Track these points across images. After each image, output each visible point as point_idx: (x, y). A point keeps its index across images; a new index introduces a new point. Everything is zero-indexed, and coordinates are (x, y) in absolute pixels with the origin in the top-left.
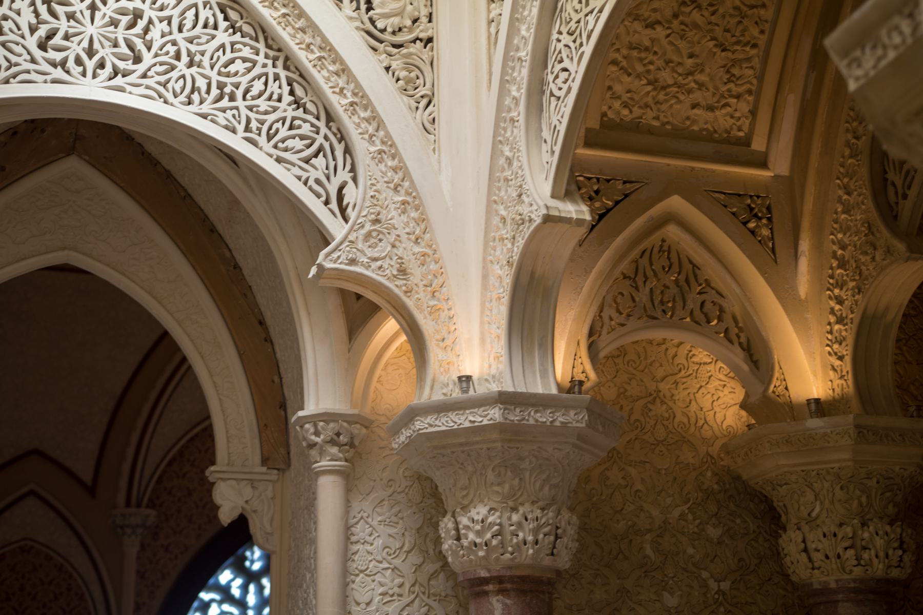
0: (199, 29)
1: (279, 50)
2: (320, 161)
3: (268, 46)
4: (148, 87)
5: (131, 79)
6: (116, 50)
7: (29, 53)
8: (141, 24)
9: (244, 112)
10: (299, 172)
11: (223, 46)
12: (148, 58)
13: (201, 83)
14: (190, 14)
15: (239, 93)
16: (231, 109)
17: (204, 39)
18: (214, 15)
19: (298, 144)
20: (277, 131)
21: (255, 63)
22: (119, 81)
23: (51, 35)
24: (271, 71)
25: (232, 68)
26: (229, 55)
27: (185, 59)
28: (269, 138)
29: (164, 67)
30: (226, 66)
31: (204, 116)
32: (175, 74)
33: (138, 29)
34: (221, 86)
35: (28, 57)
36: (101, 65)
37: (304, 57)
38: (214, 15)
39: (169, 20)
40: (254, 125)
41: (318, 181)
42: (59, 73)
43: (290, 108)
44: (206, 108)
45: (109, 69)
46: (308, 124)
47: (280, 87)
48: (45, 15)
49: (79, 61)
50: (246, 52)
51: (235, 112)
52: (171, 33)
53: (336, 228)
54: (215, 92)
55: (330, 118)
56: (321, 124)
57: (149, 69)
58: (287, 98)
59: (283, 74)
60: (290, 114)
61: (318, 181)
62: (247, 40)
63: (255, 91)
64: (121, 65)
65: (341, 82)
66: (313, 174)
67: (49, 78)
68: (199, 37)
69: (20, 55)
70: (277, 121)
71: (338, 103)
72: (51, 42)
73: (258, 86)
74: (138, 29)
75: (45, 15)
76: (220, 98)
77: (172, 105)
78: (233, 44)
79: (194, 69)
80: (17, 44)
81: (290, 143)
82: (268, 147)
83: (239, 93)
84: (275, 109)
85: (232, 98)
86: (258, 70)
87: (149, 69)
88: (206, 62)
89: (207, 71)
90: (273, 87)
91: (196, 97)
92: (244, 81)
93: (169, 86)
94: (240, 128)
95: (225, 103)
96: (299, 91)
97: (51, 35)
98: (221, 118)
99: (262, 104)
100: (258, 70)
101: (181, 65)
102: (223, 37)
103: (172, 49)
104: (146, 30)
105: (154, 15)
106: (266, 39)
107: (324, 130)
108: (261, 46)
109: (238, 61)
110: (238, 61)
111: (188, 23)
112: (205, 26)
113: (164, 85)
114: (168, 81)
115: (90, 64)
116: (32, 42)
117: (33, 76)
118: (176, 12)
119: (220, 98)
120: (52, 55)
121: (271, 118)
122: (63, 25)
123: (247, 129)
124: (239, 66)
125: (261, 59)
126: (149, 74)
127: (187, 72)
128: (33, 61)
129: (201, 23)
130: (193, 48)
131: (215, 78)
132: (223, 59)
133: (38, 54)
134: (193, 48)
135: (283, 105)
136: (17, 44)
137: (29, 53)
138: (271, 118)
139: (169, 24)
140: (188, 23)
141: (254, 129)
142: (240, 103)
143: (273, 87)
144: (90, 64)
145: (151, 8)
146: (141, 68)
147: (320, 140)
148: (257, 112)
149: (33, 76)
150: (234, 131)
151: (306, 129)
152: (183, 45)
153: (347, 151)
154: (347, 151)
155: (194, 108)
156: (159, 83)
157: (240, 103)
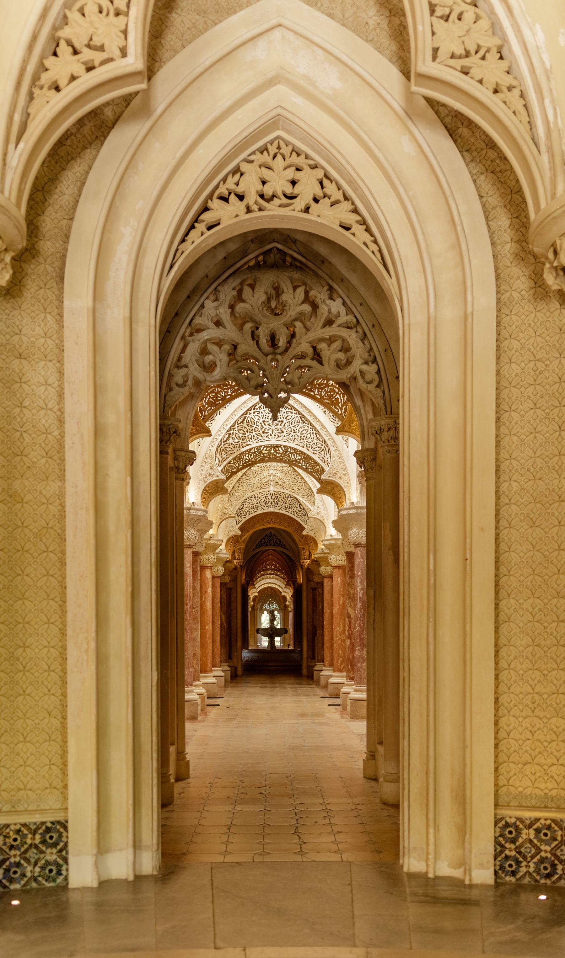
5: (282, 438)
12: (285, 432)
13: (296, 437)
15: (305, 438)
24: (312, 432)
25: (303, 432)
26: (302, 429)
27: (293, 431)
34: (301, 437)
36: (275, 436)
37: (319, 428)
42: (267, 439)
44: (298, 443)
45: (277, 436)
49: (271, 435)
50: (306, 428)
55: (325, 442)
56: (323, 443)
58: (315, 438)
59: (314, 432)
60: (316, 442)
64: (280, 435)
71: (326, 438)
73: (309, 436)
75: (263, 426)
81: (316, 449)
83: (305, 438)
85: (303, 439)
86: (309, 432)
88: (297, 431)
89: (298, 434)
90: (312, 436)
94: (305, 446)
95: (302, 441)
96: (318, 436)
98: (301, 445)
99: (310, 440)
100: (309, 432)
101: (292, 433)
103: (290, 429)
107: (324, 445)
115: (273, 435)
116: (261, 432)
117: (262, 440)
121: (311, 444)
122: (267, 427)
124: (305, 432)
125: (309, 429)
127: (294, 434)
128: (262, 436)
130: (295, 428)
131: (299, 435)
133: (263, 435)
134: (295, 428)
135: (314, 440)
138: (311, 444)
143: (312, 436)
144: (273, 435)
146: (283, 434)
147: (323, 447)
150: (303, 447)
151: (320, 445)
152: (292, 428)
155: (295, 443)
157: (305, 440)
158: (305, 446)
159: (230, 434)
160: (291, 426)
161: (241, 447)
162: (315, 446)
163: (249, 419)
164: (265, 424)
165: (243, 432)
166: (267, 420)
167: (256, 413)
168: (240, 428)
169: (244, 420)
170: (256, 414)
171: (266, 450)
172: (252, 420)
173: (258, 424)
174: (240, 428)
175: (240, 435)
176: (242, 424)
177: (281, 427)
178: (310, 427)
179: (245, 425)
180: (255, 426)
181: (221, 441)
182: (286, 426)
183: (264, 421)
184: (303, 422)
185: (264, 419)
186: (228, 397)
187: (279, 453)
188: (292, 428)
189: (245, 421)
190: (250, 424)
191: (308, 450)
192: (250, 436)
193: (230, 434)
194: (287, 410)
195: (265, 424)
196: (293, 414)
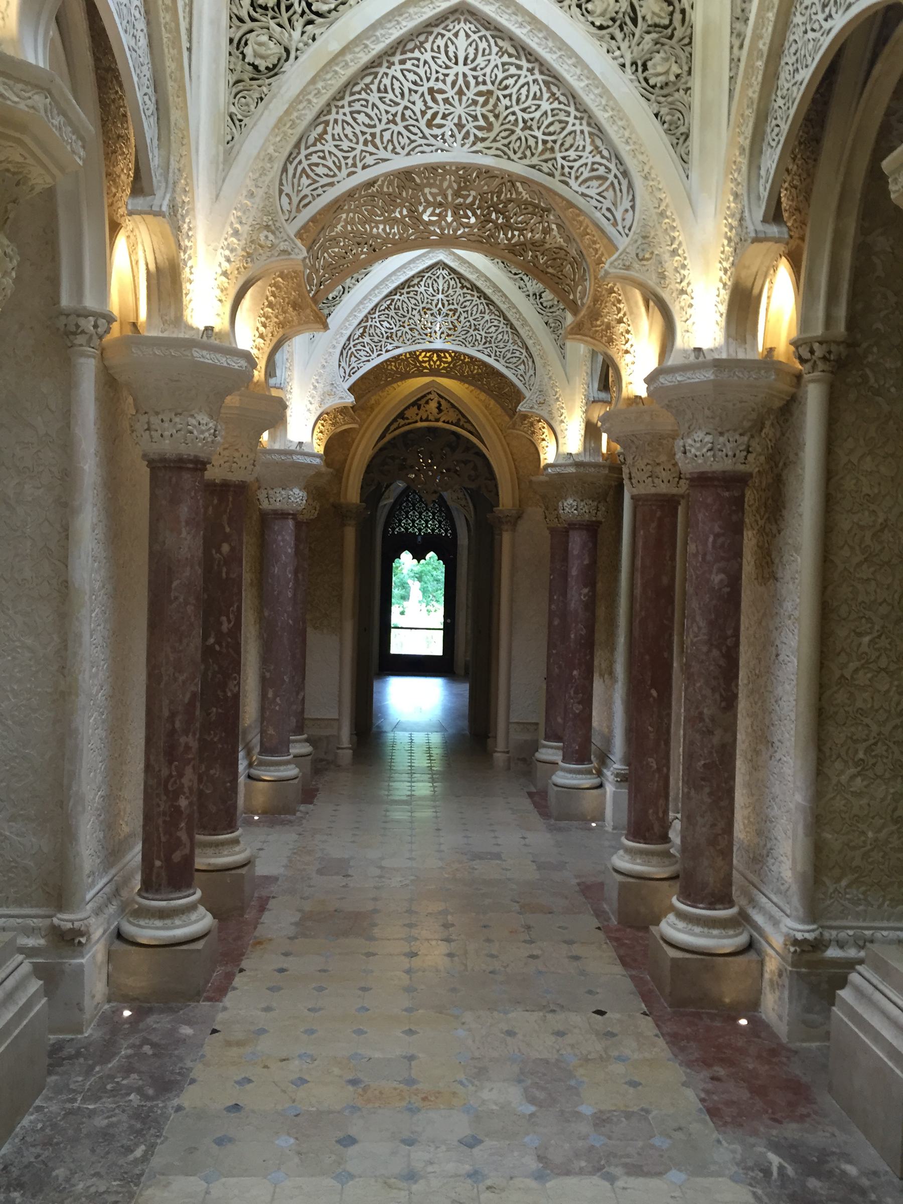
0: (478, 315)
1: (585, 111)
2: (522, 367)
3: (577, 109)
4: (497, 149)
6: (476, 123)
7: (422, 132)
8: (457, 314)
9: (495, 348)
10: (514, 371)
11: (546, 113)
13: (479, 337)
14: (475, 309)
16: (551, 159)
17: (534, 108)
18: (540, 90)
19: (514, 360)
20: (582, 173)
21: (567, 123)
22: (479, 146)
23: (435, 115)
25: (490, 330)
26: (490, 325)
27: (473, 327)
28: (504, 357)
29: (507, 133)
30: (547, 127)
31: (533, 167)
32: (469, 335)
33: (490, 107)
34: (486, 337)
35: (421, 135)
38: (540, 90)
39: (510, 95)
40: (498, 353)
41: (521, 375)
43: (590, 156)
44: (480, 348)
46: (603, 167)
47: (584, 140)
48: (430, 103)
50: (496, 323)
51: (553, 161)
52: (511, 106)
53: (527, 394)
54: (484, 340)
56: (524, 351)
57: (498, 135)
60: (512, 348)
61: (521, 375)
62: (562, 106)
63: (567, 145)
65: (530, 334)
66: (520, 372)
67: (433, 148)
68: (530, 107)
69: (416, 134)
70: (582, 166)
72: (434, 122)
73: (500, 336)
74: (456, 317)
76: (485, 343)
77: (513, 160)
78: (552, 110)
79: (476, 332)
80: (414, 126)
81: (511, 360)
82: (502, 361)
84: (581, 157)
86: (500, 330)
87: (498, 135)
89: (481, 332)
90: (506, 337)
91: (476, 343)
92: (494, 335)
93: (511, 146)
94: (493, 355)
95: (487, 345)
97: (435, 115)
98: (486, 351)
99: (501, 345)
100: (500, 330)
102: (487, 317)
103: (468, 324)
104: (459, 317)
105: (461, 310)
106: (575, 104)
108: (501, 319)
109: (556, 124)
110: (556, 124)
111: (474, 313)
112: (481, 313)
113: (507, 146)
114: (510, 143)
118: (469, 309)
119: (485, 343)
120: (436, 131)
123: (496, 356)
124: (493, 329)
126: (498, 138)
129: (531, 95)
130: (476, 323)
132: (487, 326)
134: (476, 323)
135: (509, 344)
136: (414, 126)
137: (422, 132)
138: (504, 350)
139: (510, 100)
140: (474, 313)
141: (567, 174)
142: (493, 345)
145: (498, 89)
148: (569, 161)
149: (425, 148)
150: (490, 356)
152: (473, 322)
153: (533, 362)
154: (533, 362)
155: (475, 348)
156: (504, 145)
157: (493, 345)
158: (493, 355)
159: (366, 327)
160: (470, 319)
161: (384, 350)
162: (509, 355)
163: (399, 304)
164: (434, 100)
165: (388, 326)
166: (440, 85)
167: (408, 65)
168: (383, 318)
169: (391, 304)
170: (412, 294)
171: (425, 356)
172: (405, 305)
173: (415, 312)
174: (383, 318)
175: (383, 330)
176: (387, 312)
177: (484, 110)
178: (502, 321)
179: (392, 313)
180: (409, 315)
181: (349, 339)
182: (462, 318)
183: (431, 91)
184: (491, 312)
185: (432, 83)
186: (363, 256)
187: (445, 362)
188: (520, 114)
189: (392, 307)
190: (401, 312)
191: (497, 361)
192: (399, 334)
193: (366, 327)
194: (505, 58)
195: (434, 100)
196: (524, 72)
